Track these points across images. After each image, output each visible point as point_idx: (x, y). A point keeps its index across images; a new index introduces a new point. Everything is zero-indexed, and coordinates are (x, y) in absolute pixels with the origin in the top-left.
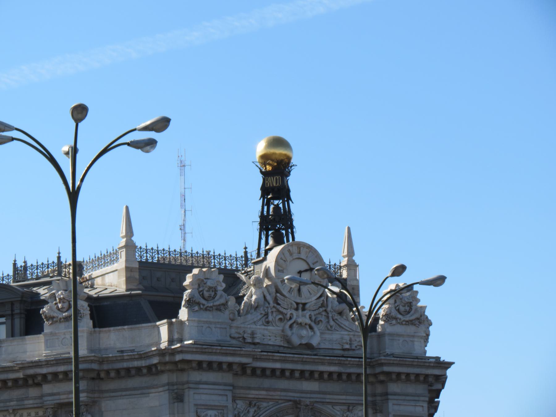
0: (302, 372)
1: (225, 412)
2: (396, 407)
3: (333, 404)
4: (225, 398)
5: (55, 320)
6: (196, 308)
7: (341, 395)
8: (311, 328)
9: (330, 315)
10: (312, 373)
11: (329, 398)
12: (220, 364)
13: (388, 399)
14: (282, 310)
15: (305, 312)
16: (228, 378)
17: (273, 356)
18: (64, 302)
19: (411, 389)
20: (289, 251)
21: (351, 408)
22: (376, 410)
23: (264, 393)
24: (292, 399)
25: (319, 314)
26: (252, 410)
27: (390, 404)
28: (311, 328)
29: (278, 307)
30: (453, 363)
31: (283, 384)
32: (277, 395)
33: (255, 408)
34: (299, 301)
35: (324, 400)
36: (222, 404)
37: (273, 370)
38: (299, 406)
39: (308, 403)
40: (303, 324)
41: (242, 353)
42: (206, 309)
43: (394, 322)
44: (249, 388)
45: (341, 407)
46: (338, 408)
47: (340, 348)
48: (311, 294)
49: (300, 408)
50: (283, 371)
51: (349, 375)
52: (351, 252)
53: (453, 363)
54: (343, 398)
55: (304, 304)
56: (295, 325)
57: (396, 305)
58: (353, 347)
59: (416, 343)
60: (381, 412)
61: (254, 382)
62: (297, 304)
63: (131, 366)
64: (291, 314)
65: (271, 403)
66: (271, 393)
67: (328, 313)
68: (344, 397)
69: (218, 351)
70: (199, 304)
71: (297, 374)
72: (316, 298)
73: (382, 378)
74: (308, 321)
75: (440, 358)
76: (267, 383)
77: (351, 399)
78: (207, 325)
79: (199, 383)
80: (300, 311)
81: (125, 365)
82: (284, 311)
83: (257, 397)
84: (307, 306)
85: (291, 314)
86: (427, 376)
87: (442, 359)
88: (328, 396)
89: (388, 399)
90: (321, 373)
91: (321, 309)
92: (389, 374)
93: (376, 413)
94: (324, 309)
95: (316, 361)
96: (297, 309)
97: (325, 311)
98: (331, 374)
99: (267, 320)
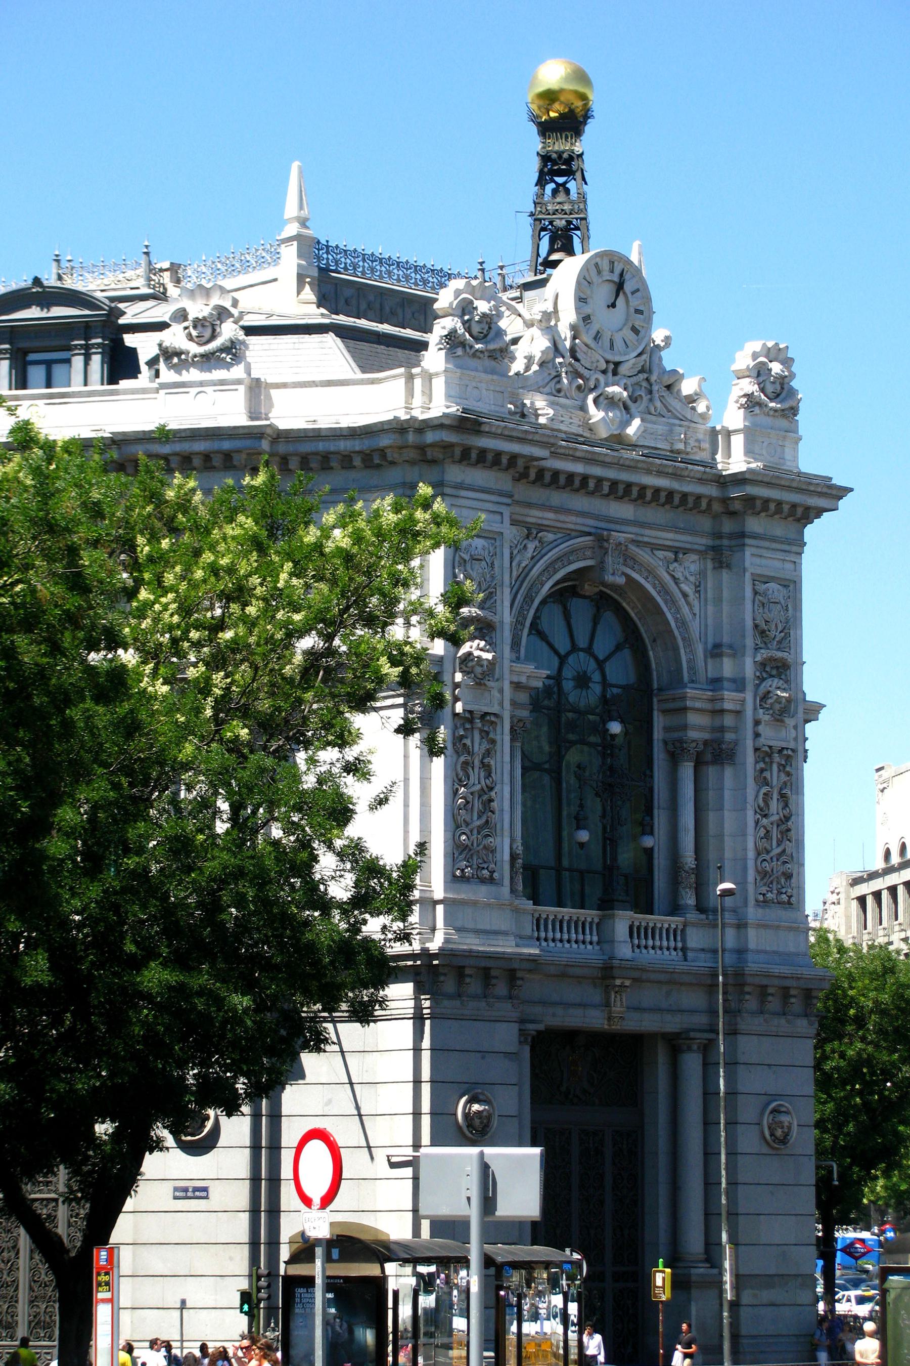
0: (614, 484)
1: (498, 543)
2: (758, 561)
3: (654, 547)
4: (498, 517)
5: (183, 357)
6: (459, 351)
7: (668, 531)
8: (626, 408)
9: (655, 388)
10: (629, 486)
11: (650, 535)
12: (498, 454)
13: (744, 545)
14: (582, 370)
15: (616, 378)
17: (576, 449)
18: (203, 326)
19: (779, 528)
20: (596, 265)
21: (681, 556)
22: (721, 562)
23: (551, 515)
24: (593, 530)
25: (637, 384)
26: (531, 546)
27: (748, 552)
28: (626, 408)
29: (577, 364)
30: (851, 490)
31: (580, 502)
32: (571, 522)
33: (537, 543)
34: (610, 357)
35: (640, 539)
36: (495, 529)
37: (571, 476)
38: (606, 544)
39: (622, 540)
40: (616, 400)
41: (537, 438)
43: (757, 410)
44: (529, 505)
45: (666, 553)
46: (660, 554)
47: (668, 448)
48: (627, 346)
49: (607, 549)
50: (585, 478)
51: (685, 496)
52: (556, 304)
53: (851, 490)
54: (667, 538)
55: (617, 364)
56: (602, 398)
57: (761, 379)
58: (689, 450)
59: (787, 450)
60: (729, 567)
61: (537, 494)
62: (607, 362)
63: (332, 449)
64: (597, 379)
65: (560, 535)
66: (562, 517)
67: (651, 385)
68: (671, 535)
69: (499, 431)
70: (463, 344)
72: (635, 354)
73: (737, 506)
75: (831, 479)
76: (557, 498)
77: (683, 540)
78: (474, 384)
79: (460, 486)
80: (610, 374)
81: (321, 446)
82: (586, 373)
83: (540, 522)
84: (623, 369)
85: (597, 379)
86: (808, 509)
87: (833, 482)
88: (647, 532)
89: (744, 545)
90: (643, 488)
91: (642, 376)
92: (749, 500)
93: (722, 567)
94: (645, 375)
95: (640, 465)
96: (604, 372)
97: (647, 379)
98: (657, 491)
99: (558, 386)
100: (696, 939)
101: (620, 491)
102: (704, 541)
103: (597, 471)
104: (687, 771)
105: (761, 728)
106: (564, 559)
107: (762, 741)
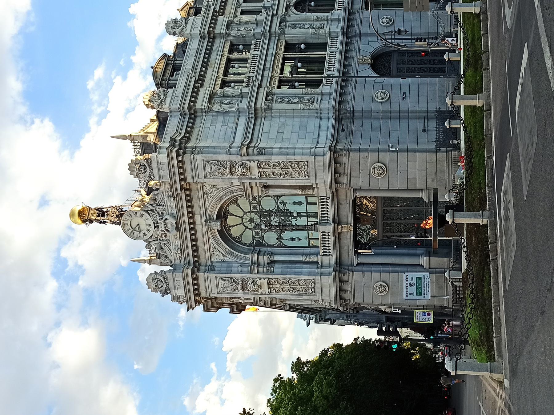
8: (166, 219)
10: (190, 224)
11: (203, 209)
16: (201, 275)
19: (188, 168)
28: (166, 219)
32: (206, 239)
34: (153, 227)
37: (193, 246)
42: (168, 285)
62: (155, 227)
68: (201, 200)
71: (193, 232)
74: (163, 223)
76: (200, 244)
77: (201, 194)
88: (202, 209)
96: (158, 227)
100: (323, 193)
101: (192, 226)
102: (199, 186)
103: (189, 239)
104: (270, 191)
105: (253, 177)
106: (217, 243)
107: (257, 176)
